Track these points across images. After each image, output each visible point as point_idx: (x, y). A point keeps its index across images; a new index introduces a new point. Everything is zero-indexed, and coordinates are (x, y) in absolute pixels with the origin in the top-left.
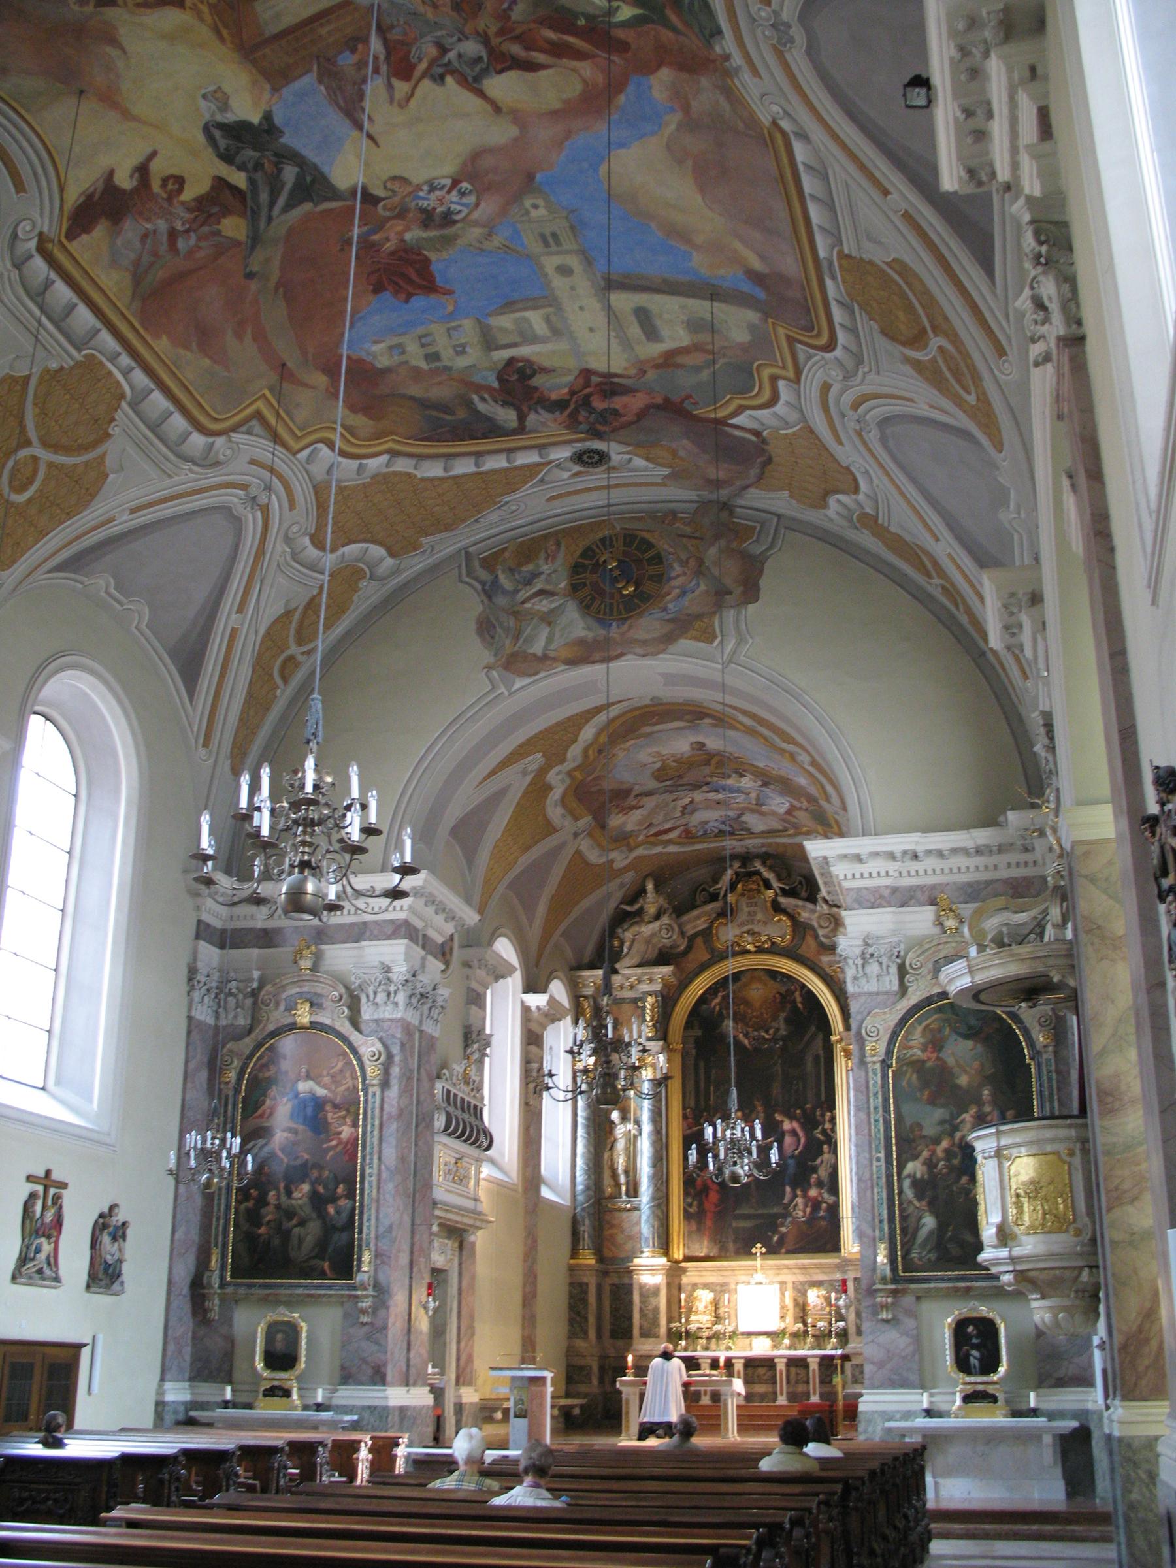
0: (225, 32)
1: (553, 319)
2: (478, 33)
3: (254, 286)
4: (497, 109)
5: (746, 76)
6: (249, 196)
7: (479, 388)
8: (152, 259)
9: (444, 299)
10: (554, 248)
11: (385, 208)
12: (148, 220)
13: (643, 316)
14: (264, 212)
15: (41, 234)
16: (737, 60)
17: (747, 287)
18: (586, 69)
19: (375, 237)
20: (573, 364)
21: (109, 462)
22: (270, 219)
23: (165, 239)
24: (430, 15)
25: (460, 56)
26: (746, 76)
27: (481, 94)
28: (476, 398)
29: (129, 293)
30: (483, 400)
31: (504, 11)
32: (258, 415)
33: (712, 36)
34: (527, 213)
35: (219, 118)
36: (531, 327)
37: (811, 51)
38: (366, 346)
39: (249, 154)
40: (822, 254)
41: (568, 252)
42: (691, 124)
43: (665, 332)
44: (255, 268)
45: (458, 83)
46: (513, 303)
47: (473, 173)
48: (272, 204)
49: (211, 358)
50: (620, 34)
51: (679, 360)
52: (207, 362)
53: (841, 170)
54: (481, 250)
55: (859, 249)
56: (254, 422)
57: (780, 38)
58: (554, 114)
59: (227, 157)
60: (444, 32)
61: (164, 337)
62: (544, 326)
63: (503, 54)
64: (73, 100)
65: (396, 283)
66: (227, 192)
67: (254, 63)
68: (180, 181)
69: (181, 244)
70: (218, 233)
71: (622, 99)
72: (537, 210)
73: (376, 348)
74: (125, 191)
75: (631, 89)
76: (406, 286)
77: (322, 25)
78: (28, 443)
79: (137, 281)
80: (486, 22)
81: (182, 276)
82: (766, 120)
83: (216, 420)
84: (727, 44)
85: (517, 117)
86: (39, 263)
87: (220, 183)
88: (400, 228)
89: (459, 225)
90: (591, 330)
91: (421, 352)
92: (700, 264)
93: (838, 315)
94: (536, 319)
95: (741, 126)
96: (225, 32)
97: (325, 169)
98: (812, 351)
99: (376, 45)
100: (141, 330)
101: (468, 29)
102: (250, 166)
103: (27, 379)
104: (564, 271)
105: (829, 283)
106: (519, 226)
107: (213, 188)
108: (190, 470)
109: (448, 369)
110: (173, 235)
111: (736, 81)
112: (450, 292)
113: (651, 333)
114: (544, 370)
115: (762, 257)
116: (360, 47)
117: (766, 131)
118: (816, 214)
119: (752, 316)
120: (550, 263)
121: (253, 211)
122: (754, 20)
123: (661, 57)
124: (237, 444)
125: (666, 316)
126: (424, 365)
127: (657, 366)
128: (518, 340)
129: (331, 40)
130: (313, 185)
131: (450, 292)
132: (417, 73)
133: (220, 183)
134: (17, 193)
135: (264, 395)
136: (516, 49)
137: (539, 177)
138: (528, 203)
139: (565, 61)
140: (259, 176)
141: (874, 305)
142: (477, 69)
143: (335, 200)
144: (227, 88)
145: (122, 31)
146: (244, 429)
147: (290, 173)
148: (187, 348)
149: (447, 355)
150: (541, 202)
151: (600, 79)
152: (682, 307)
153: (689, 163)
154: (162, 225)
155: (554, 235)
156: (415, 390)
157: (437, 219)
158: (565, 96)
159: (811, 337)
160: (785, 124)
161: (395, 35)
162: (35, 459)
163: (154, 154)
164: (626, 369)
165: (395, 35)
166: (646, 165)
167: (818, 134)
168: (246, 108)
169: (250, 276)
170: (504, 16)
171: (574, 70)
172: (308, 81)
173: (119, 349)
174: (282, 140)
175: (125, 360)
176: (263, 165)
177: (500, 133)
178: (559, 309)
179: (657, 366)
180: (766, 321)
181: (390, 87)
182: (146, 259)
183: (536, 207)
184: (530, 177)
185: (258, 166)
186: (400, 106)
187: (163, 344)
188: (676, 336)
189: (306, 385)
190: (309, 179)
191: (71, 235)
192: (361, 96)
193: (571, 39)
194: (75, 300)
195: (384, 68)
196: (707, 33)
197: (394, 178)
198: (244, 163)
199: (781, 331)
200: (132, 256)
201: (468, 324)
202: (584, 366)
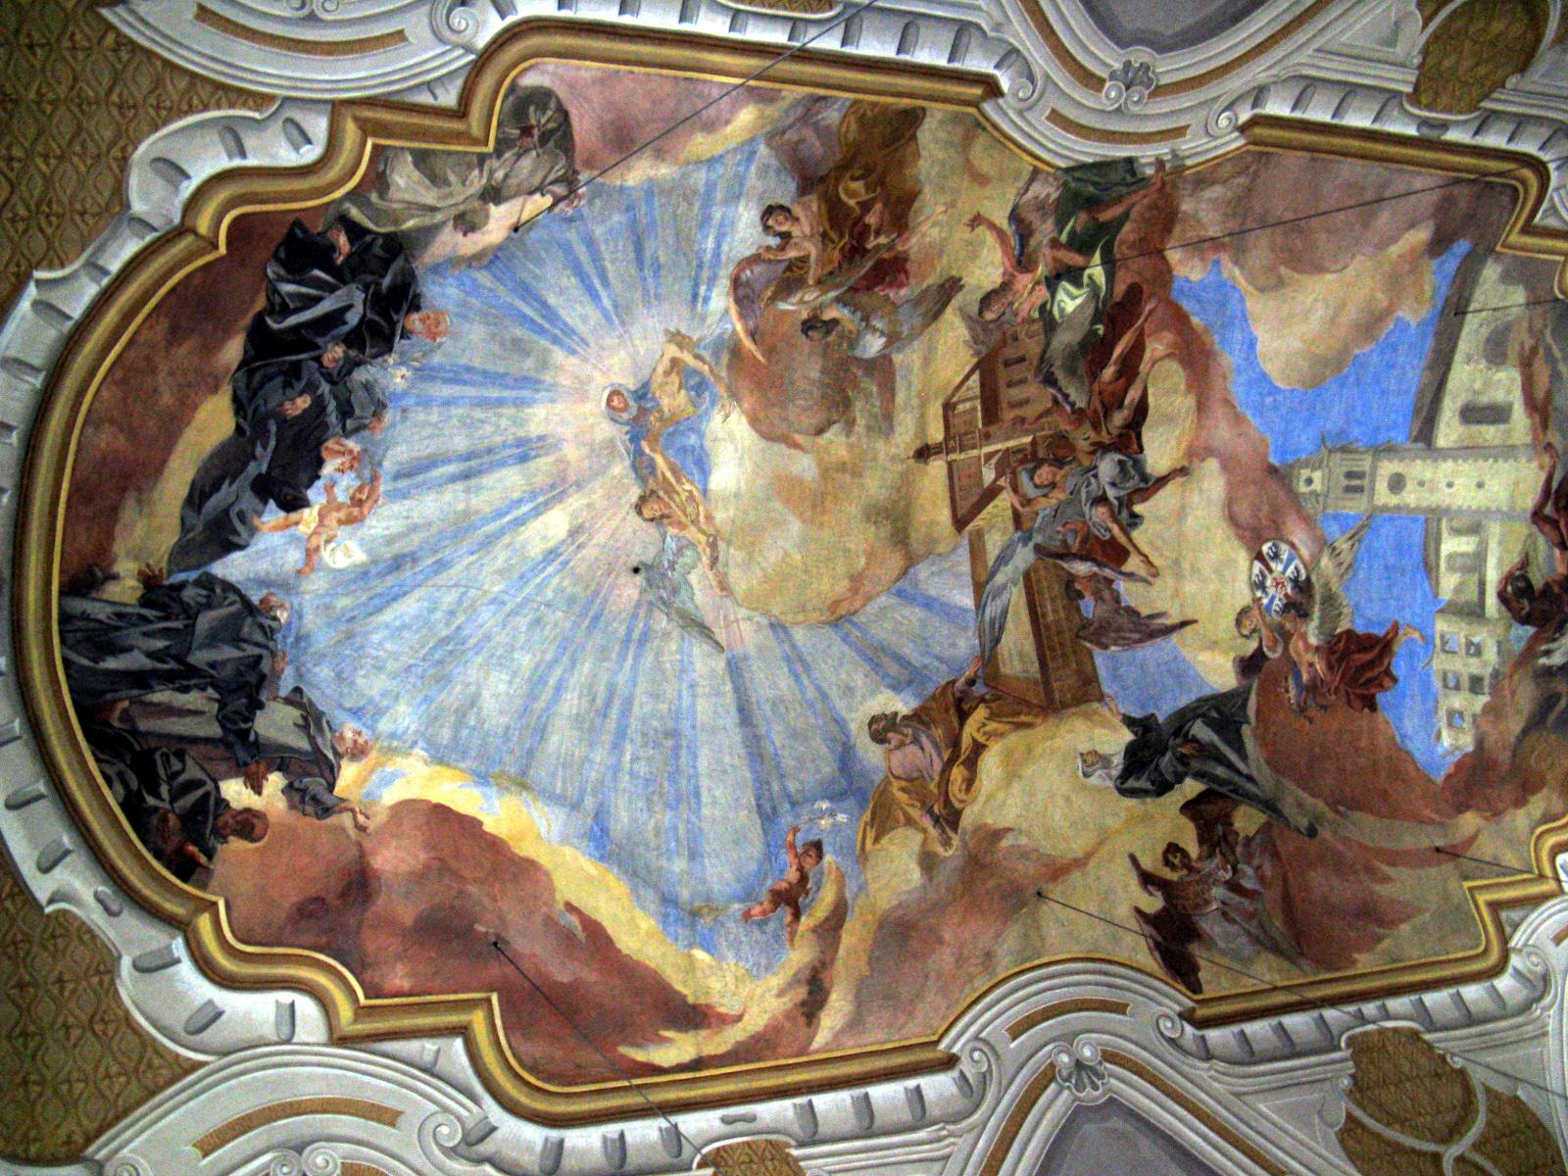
0: (1023, 718)
1: (1455, 524)
2: (1093, 453)
3: (1325, 833)
4: (1182, 471)
5: (1185, 145)
6: (1215, 787)
7: (1529, 653)
8: (1255, 922)
9: (1401, 638)
10: (1366, 482)
11: (1271, 649)
12: (1207, 902)
13: (1472, 414)
14: (1242, 782)
15: (1181, 1015)
16: (1162, 150)
17: (1451, 262)
18: (1155, 348)
19: (1305, 677)
20: (1523, 528)
21: (1500, 1085)
22: (1250, 778)
23: (1236, 898)
24: (1062, 496)
25: (1113, 484)
26: (1185, 145)
27: (1162, 481)
28: (1543, 661)
29: (1286, 964)
30: (1548, 653)
31: (1074, 412)
32: (1495, 907)
33: (1133, 173)
34: (1314, 493)
35: (1115, 773)
36: (1462, 555)
37: (1163, 47)
38: (1440, 750)
39: (1166, 761)
40: (1411, 131)
41: (1374, 468)
42: (1234, 242)
43: (1499, 396)
44: (1303, 823)
45: (1144, 500)
46: (1426, 564)
47: (1257, 534)
48: (1230, 766)
49: (1401, 921)
50: (1120, 288)
51: (1540, 393)
52: (1405, 928)
53: (1301, 55)
54: (1350, 566)
55: (1403, 65)
56: (1504, 915)
57: (1141, 83)
58: (1201, 407)
59: (1162, 788)
60: (1084, 491)
61: (1356, 956)
62: (1464, 539)
63: (1120, 436)
64: (1046, 908)
65: (1370, 681)
66: (1203, 807)
67: (1065, 706)
68: (1172, 848)
69: (1249, 884)
70: (1248, 841)
71: (1195, 320)
72: (1313, 481)
73: (1447, 740)
74: (1164, 909)
75: (1186, 305)
76: (1376, 671)
77: (1044, 615)
78: (1436, 1158)
79: (1275, 949)
80: (1083, 437)
81: (1287, 899)
82: (1236, 142)
83: (1486, 951)
84: (1146, 154)
85: (1197, 452)
86: (1213, 1035)
87: (1190, 808)
88: (1301, 644)
89: (1314, 578)
90: (1480, 485)
91: (1465, 694)
92: (1414, 314)
93: (1495, 139)
94: (1452, 545)
95: (1242, 180)
96: (1023, 718)
97: (1207, 692)
98: (1545, 205)
99: (1082, 568)
100: (1338, 974)
101: (1086, 462)
102: (1180, 769)
103: (1350, 1117)
104: (1397, 483)
105: (1452, 136)
106: (1330, 511)
107: (1193, 819)
108: (1544, 1009)
109: (1496, 674)
110: (1234, 886)
111: (1189, 162)
112: (1395, 628)
113: (1497, 414)
114: (1525, 563)
115: (1412, 225)
116: (1078, 586)
117: (1251, 147)
118: (1359, 119)
119: (1491, 272)
120: (1383, 496)
121: (1235, 791)
122: (1118, 110)
123: (1153, 250)
124: (1525, 945)
125: (1477, 385)
126: (1483, 700)
127: (1545, 425)
128: (1476, 577)
129: (1062, 614)
130: (1223, 712)
131: (1395, 628)
132: (1122, 539)
133: (1190, 808)
134: (1124, 1013)
135: (1471, 889)
136: (1119, 418)
137: (1273, 460)
138: (1303, 488)
139: (1143, 367)
140: (1195, 765)
141: (1482, 71)
142: (1133, 472)
143: (1247, 699)
144: (1084, 747)
145: (990, 821)
146: (1508, 930)
147: (1200, 730)
148: (1379, 939)
149: (1474, 666)
150: (1305, 473)
151: (1168, 336)
152: (1469, 360)
153: (1283, 270)
154: (1218, 892)
155: (1349, 475)
156: (1515, 725)
157: (1299, 598)
158: (1183, 387)
159: (1526, 191)
160: (1244, 116)
161: (1075, 544)
162: (1460, 1160)
163: (1133, 859)
164: (1541, 467)
165: (1075, 544)
166: (1281, 326)
167: (1257, 72)
168: (1116, 741)
169: (1312, 832)
170: (1079, 415)
171: (1154, 363)
172: (1100, 658)
173: (1352, 1008)
174: (1161, 719)
175: (1370, 1008)
176: (1183, 755)
177: (1211, 482)
178: (1447, 511)
179: (1545, 425)
180: (1500, 254)
181: (1130, 576)
182: (1252, 927)
183: (1309, 481)
184: (1272, 471)
185: (1182, 759)
186: (1156, 575)
187: (1365, 962)
188: (1505, 385)
189: (1474, 837)
190: (1214, 714)
191: (1195, 987)
192: (1132, 612)
193: (1118, 351)
194: (1274, 1021)
195: (1108, 572)
196: (1129, 179)
197: (1239, 623)
198: (1175, 773)
199: (1514, 238)
200: (1244, 939)
201: (1441, 626)
202: (1528, 515)
